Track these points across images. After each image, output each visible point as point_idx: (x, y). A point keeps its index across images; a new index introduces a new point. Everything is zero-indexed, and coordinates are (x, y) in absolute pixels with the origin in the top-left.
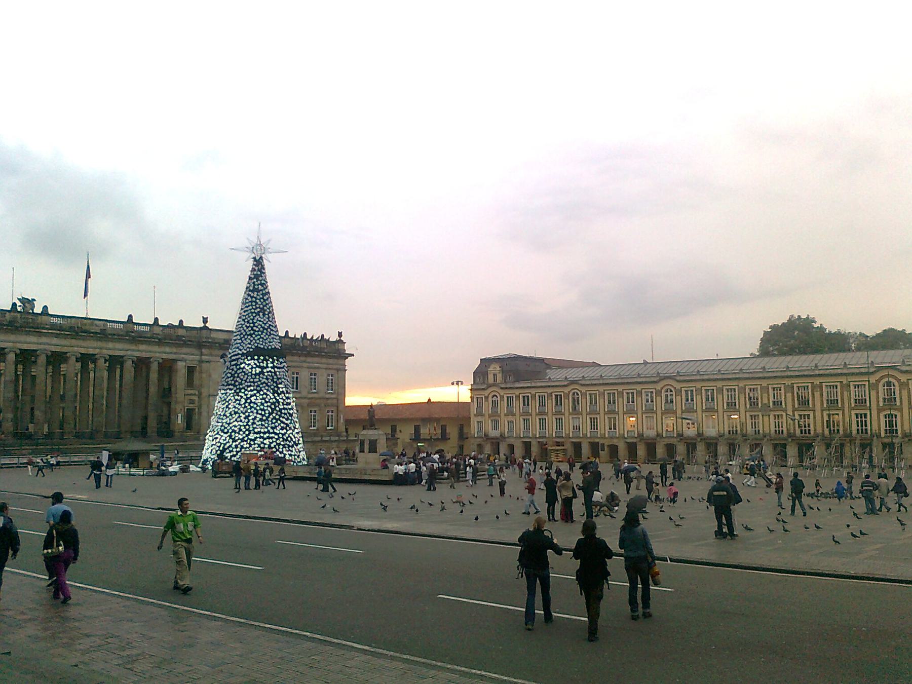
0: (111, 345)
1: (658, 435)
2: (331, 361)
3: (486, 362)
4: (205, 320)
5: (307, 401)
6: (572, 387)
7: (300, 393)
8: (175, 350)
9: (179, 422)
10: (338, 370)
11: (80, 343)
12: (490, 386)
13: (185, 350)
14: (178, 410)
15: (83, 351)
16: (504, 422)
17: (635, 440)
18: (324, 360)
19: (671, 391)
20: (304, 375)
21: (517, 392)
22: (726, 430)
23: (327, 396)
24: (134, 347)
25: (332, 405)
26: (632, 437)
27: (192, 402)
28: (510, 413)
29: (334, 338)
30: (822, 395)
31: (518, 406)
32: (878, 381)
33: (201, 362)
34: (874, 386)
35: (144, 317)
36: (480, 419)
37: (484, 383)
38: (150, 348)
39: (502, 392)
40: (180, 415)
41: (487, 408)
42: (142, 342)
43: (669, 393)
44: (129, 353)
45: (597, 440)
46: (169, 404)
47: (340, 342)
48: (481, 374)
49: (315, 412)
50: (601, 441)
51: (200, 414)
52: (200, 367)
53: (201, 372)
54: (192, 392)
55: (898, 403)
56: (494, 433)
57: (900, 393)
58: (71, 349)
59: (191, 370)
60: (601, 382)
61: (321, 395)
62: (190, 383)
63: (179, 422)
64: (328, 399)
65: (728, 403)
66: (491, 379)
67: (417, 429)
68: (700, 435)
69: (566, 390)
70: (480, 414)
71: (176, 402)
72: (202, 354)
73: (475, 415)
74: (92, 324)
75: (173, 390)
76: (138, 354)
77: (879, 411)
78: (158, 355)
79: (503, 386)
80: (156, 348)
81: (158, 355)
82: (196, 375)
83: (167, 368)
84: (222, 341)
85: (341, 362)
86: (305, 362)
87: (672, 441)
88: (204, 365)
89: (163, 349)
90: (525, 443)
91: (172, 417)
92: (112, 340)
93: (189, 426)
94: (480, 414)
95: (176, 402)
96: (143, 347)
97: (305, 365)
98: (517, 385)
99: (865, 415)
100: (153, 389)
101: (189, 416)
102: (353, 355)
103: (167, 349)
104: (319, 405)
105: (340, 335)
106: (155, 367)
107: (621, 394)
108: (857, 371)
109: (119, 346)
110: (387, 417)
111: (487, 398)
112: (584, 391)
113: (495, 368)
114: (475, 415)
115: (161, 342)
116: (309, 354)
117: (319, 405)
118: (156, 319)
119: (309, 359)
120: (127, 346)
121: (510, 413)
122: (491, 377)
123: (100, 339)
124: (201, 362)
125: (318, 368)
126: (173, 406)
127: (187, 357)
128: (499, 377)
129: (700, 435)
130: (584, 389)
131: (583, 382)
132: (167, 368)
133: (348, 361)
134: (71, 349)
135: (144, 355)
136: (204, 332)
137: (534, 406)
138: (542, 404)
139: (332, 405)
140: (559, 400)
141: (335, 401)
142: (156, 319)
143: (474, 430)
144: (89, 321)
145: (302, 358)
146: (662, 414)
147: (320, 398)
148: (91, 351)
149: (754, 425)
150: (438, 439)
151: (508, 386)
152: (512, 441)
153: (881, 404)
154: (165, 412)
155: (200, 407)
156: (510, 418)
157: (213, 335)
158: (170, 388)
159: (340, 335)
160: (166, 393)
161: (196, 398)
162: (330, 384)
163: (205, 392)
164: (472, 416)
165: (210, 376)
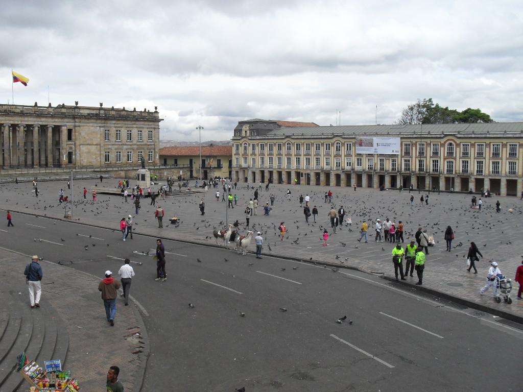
0: (26, 119)
1: (331, 170)
2: (151, 123)
3: (241, 123)
4: (77, 103)
6: (288, 139)
7: (132, 142)
8: (60, 120)
9: (65, 159)
10: (154, 128)
11: (10, 118)
12: (243, 138)
13: (66, 120)
14: (64, 153)
15: (12, 122)
16: (250, 159)
17: (319, 171)
18: (146, 123)
19: (339, 144)
20: (135, 132)
21: (257, 142)
22: (367, 167)
23: (149, 143)
24: (39, 119)
26: (318, 169)
27: (71, 148)
28: (254, 154)
29: (153, 110)
30: (416, 149)
31: (258, 150)
32: (445, 142)
33: (75, 126)
34: (443, 145)
35: (43, 103)
36: (237, 156)
37: (240, 136)
38: (47, 120)
39: (249, 142)
40: (65, 156)
41: (241, 150)
42: (43, 117)
43: (338, 145)
44: (36, 123)
46: (59, 149)
47: (156, 112)
48: (238, 131)
49: (141, 152)
50: (302, 172)
51: (75, 155)
52: (75, 129)
53: (75, 132)
54: (71, 143)
55: (454, 155)
56: (244, 165)
57: (456, 150)
58: (5, 122)
59: (70, 131)
60: (302, 137)
61: (145, 142)
62: (70, 138)
63: (65, 159)
64: (149, 145)
66: (243, 134)
67: (204, 162)
69: (284, 141)
71: (62, 149)
72: (75, 122)
73: (235, 155)
74: (16, 108)
75: (61, 142)
76: (41, 123)
77: (445, 159)
78: (51, 123)
79: (250, 138)
80: (50, 120)
81: (51, 123)
82: (73, 134)
83: (57, 130)
84: (86, 115)
85: (156, 123)
86: (135, 124)
87: (339, 172)
88: (77, 128)
89: (54, 120)
91: (61, 156)
92: (27, 116)
93: (70, 161)
95: (62, 149)
96: (43, 119)
97: (135, 126)
98: (258, 138)
99: (437, 161)
100: (50, 142)
101: (70, 155)
102: (163, 120)
103: (56, 120)
105: (156, 108)
106: (50, 130)
107: (313, 144)
108: (435, 136)
109: (30, 119)
111: (241, 144)
113: (246, 128)
114: (235, 155)
115: (53, 117)
116: (137, 120)
118: (50, 104)
119: (137, 123)
120: (35, 119)
121: (254, 154)
122: (243, 133)
123: (21, 116)
124: (75, 126)
126: (61, 150)
127: (66, 125)
128: (248, 132)
129: (353, 169)
130: (293, 141)
131: (293, 137)
132: (57, 130)
133: (160, 123)
134: (5, 122)
135: (44, 124)
136: (76, 110)
137: (267, 149)
140: (280, 146)
141: (153, 146)
142: (50, 104)
143: (234, 163)
144: (14, 107)
145: (134, 122)
147: (144, 145)
148: (16, 123)
149: (382, 165)
150: (215, 168)
152: (254, 170)
153: (446, 155)
154: (57, 154)
155: (75, 151)
157: (82, 111)
158: (59, 141)
159: (156, 108)
160: (57, 144)
161: (73, 146)
162: (150, 137)
163: (78, 143)
164: (233, 154)
165: (80, 134)
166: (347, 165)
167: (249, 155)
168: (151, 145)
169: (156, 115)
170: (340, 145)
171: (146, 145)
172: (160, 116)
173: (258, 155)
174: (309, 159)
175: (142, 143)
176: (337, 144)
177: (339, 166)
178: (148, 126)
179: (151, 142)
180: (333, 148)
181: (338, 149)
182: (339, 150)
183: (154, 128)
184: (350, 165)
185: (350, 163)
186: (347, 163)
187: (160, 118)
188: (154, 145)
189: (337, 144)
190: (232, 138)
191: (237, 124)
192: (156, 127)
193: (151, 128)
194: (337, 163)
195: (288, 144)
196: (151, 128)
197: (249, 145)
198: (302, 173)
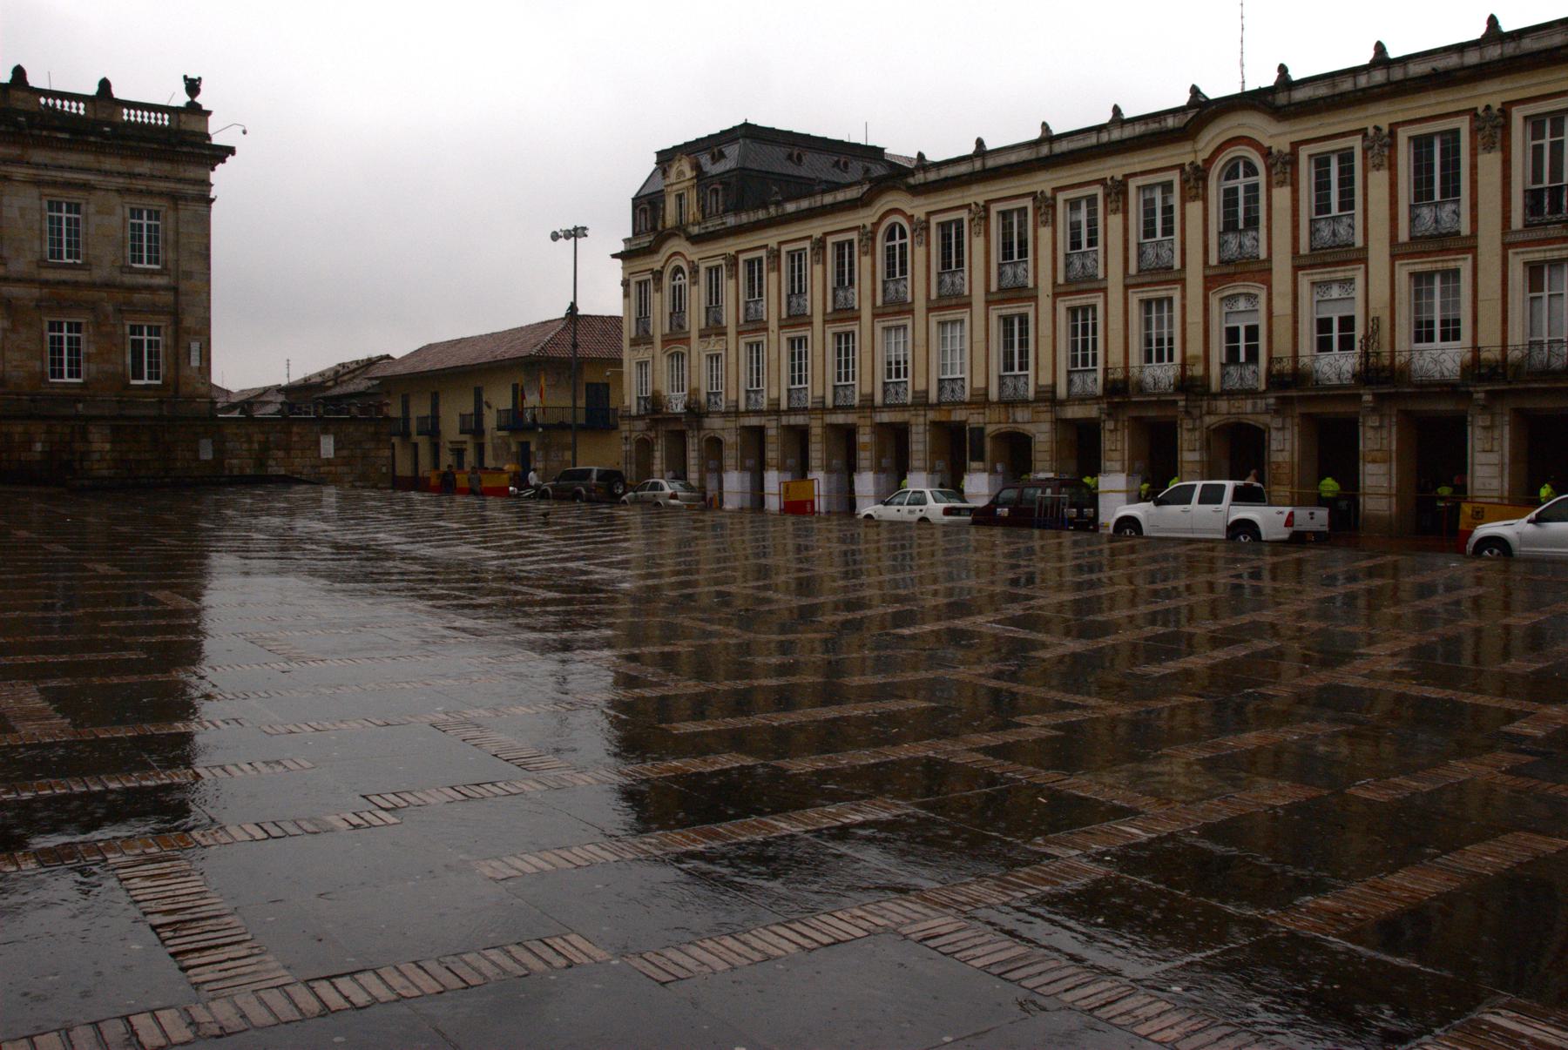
2: (144, 167)
5: (35, 292)
12: (663, 237)
16: (698, 350)
17: (1092, 411)
18: (110, 163)
19: (1251, 170)
23: (128, 279)
25: (155, 310)
26: (1083, 399)
28: (714, 328)
39: (693, 253)
41: (660, 304)
43: (1241, 183)
45: (958, 415)
47: (194, 110)
49: (76, 327)
61: (99, 274)
64: (134, 289)
65: (1534, 199)
66: (671, 217)
68: (1368, 375)
69: (866, 217)
70: (643, 338)
79: (695, 230)
85: (193, 172)
90: (791, 428)
94: (643, 338)
104: (93, 307)
105: (193, 86)
110: (489, 358)
112: (920, 214)
114: (635, 343)
117: (93, 307)
119: (39, 156)
121: (714, 328)
122: (671, 204)
125: (86, 187)
128: (692, 197)
130: (918, 207)
133: (220, 176)
138: (797, 289)
139: (155, 310)
141: (167, 298)
146: (1210, 282)
147: (92, 285)
151: (713, 225)
152: (714, 424)
156: (715, 346)
159: (193, 86)
166: (1324, 345)
167: (694, 335)
168: (149, 288)
169: (190, 124)
170: (1261, 179)
171: (107, 285)
172: (219, 136)
173: (731, 331)
174: (1024, 319)
175: (82, 276)
176: (1231, 173)
177: (1252, 354)
178: (121, 182)
179: (153, 273)
180: (1195, 208)
181: (1240, 217)
182: (1252, 222)
183: (175, 198)
184: (1346, 344)
185: (1347, 323)
186: (1324, 325)
187: (217, 140)
188: (175, 290)
189: (1231, 173)
190: (621, 248)
191: (650, 164)
192: (191, 190)
193: (150, 193)
194: (1232, 334)
195: (891, 237)
196: (150, 193)
197: (694, 270)
198: (979, 432)
